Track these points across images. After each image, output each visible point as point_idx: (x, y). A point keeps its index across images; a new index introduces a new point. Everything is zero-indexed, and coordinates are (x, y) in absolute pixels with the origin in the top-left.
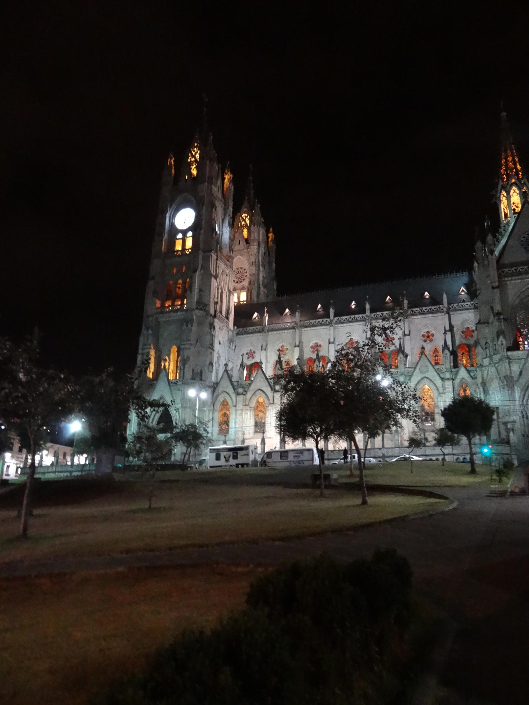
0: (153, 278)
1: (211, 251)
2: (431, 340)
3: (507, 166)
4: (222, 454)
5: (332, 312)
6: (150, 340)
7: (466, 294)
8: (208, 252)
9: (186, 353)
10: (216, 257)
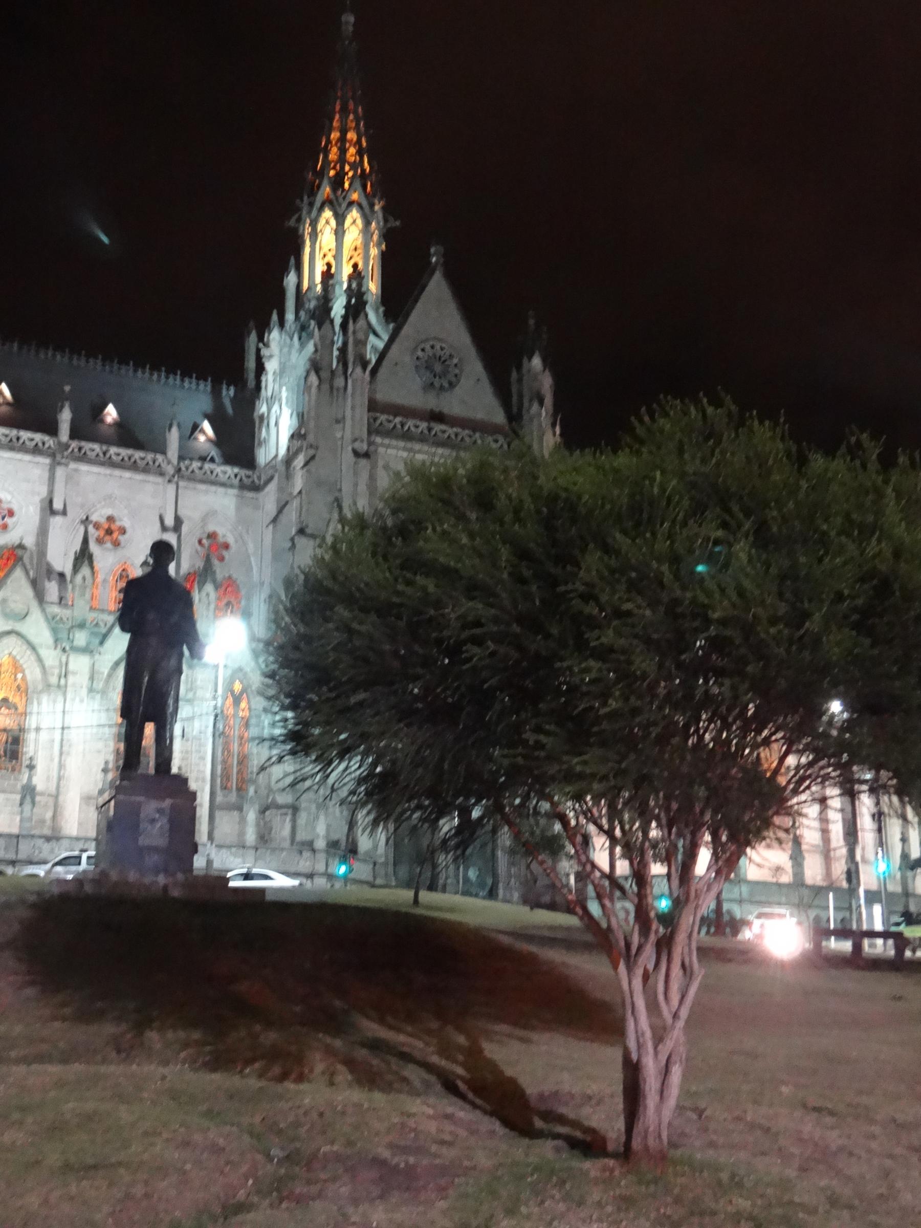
2: (116, 544)
3: (343, 151)
7: (209, 440)
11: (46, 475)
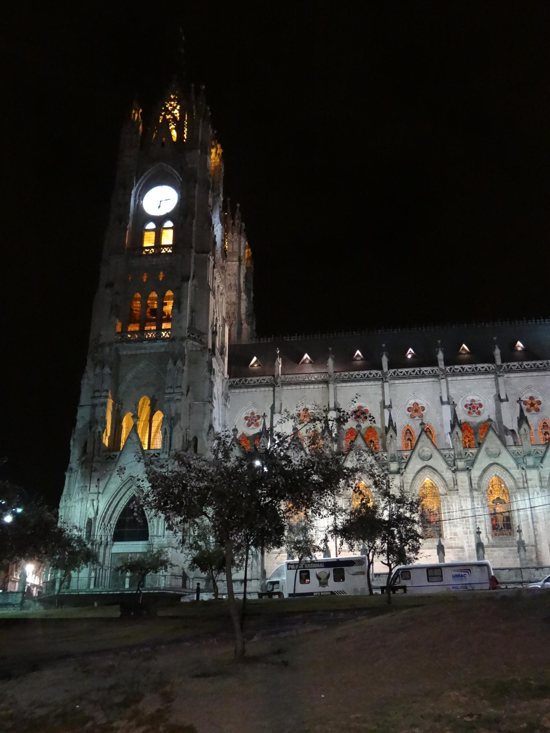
0: (110, 285)
1: (208, 252)
2: (538, 410)
4: (313, 572)
5: (385, 361)
6: (108, 384)
8: (204, 253)
9: (174, 407)
10: (213, 262)
11: (494, 383)
